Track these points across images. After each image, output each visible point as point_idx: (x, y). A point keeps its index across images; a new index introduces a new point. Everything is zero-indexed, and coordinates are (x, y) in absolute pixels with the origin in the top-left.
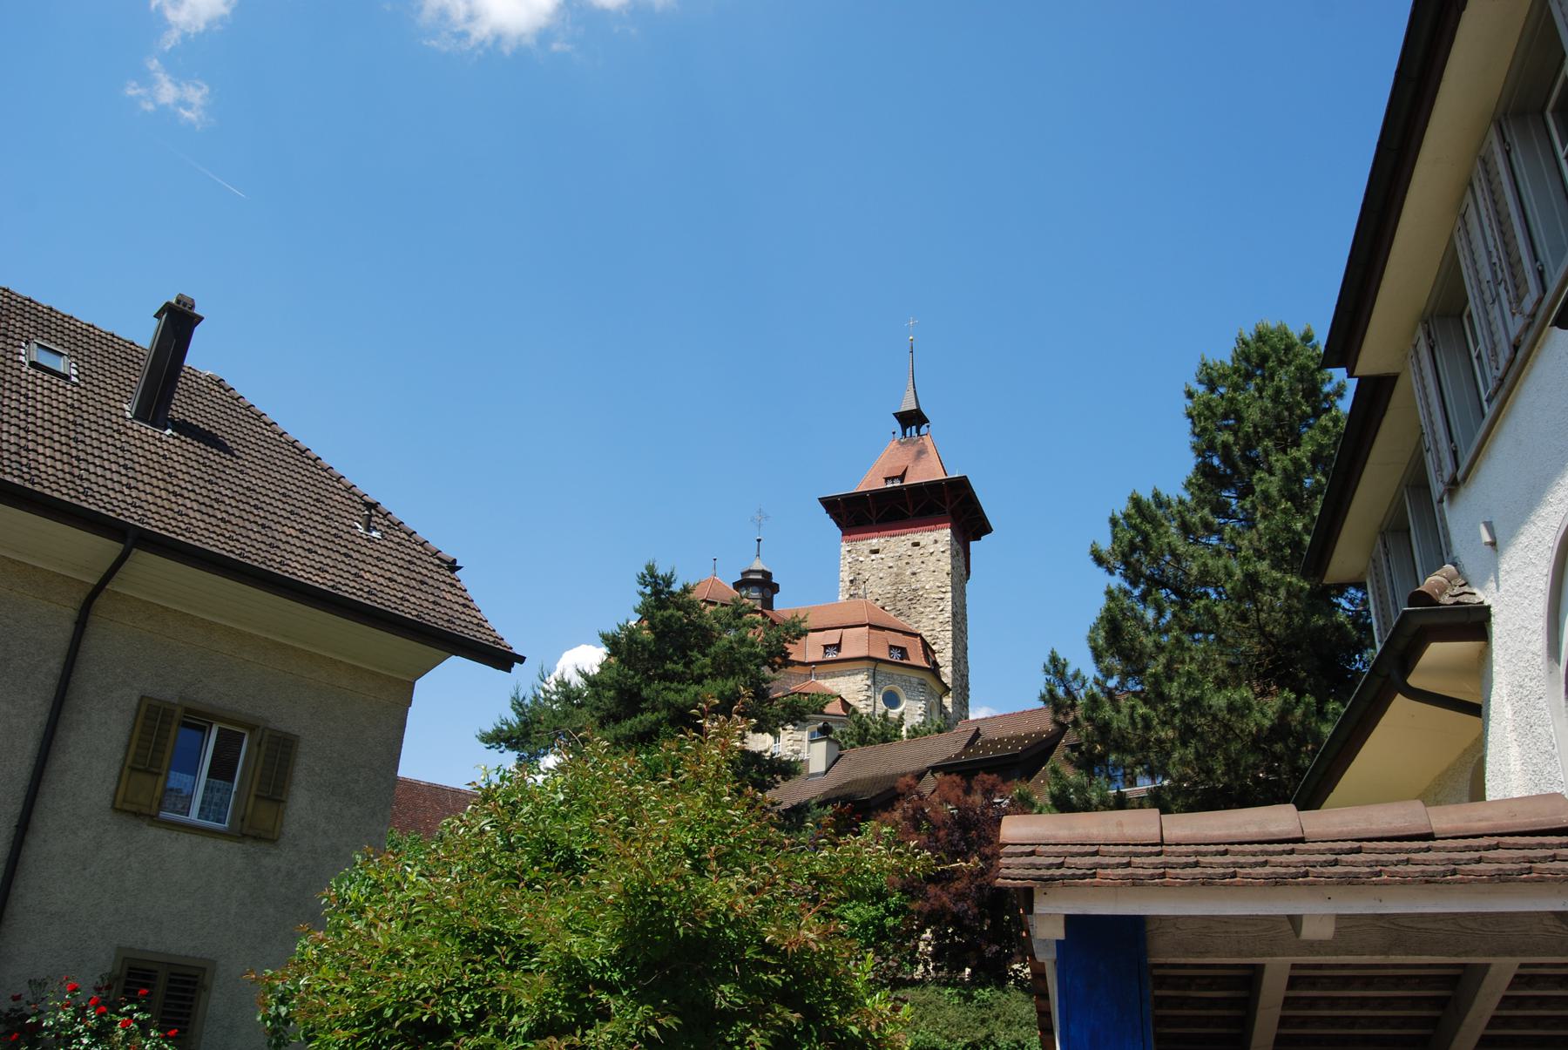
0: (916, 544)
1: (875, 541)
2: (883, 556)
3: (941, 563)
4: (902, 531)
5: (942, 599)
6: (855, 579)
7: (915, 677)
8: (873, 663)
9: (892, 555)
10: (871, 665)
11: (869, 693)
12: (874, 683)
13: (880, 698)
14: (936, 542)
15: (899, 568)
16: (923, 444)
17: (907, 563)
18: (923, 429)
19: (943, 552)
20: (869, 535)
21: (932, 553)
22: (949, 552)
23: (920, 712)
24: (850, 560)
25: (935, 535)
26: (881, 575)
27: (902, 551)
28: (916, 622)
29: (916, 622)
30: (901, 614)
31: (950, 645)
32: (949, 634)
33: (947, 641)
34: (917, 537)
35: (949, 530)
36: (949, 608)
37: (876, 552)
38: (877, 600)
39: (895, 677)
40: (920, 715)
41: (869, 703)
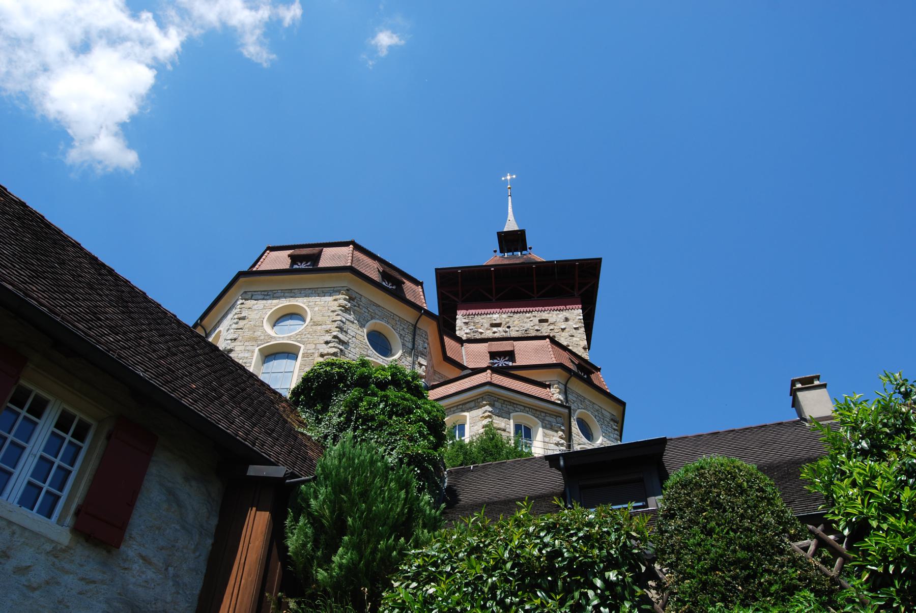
1: (495, 316)
3: (574, 339)
8: (565, 373)
14: (567, 320)
19: (575, 329)
21: (563, 330)
24: (468, 331)
25: (565, 314)
34: (545, 315)
35: (581, 311)
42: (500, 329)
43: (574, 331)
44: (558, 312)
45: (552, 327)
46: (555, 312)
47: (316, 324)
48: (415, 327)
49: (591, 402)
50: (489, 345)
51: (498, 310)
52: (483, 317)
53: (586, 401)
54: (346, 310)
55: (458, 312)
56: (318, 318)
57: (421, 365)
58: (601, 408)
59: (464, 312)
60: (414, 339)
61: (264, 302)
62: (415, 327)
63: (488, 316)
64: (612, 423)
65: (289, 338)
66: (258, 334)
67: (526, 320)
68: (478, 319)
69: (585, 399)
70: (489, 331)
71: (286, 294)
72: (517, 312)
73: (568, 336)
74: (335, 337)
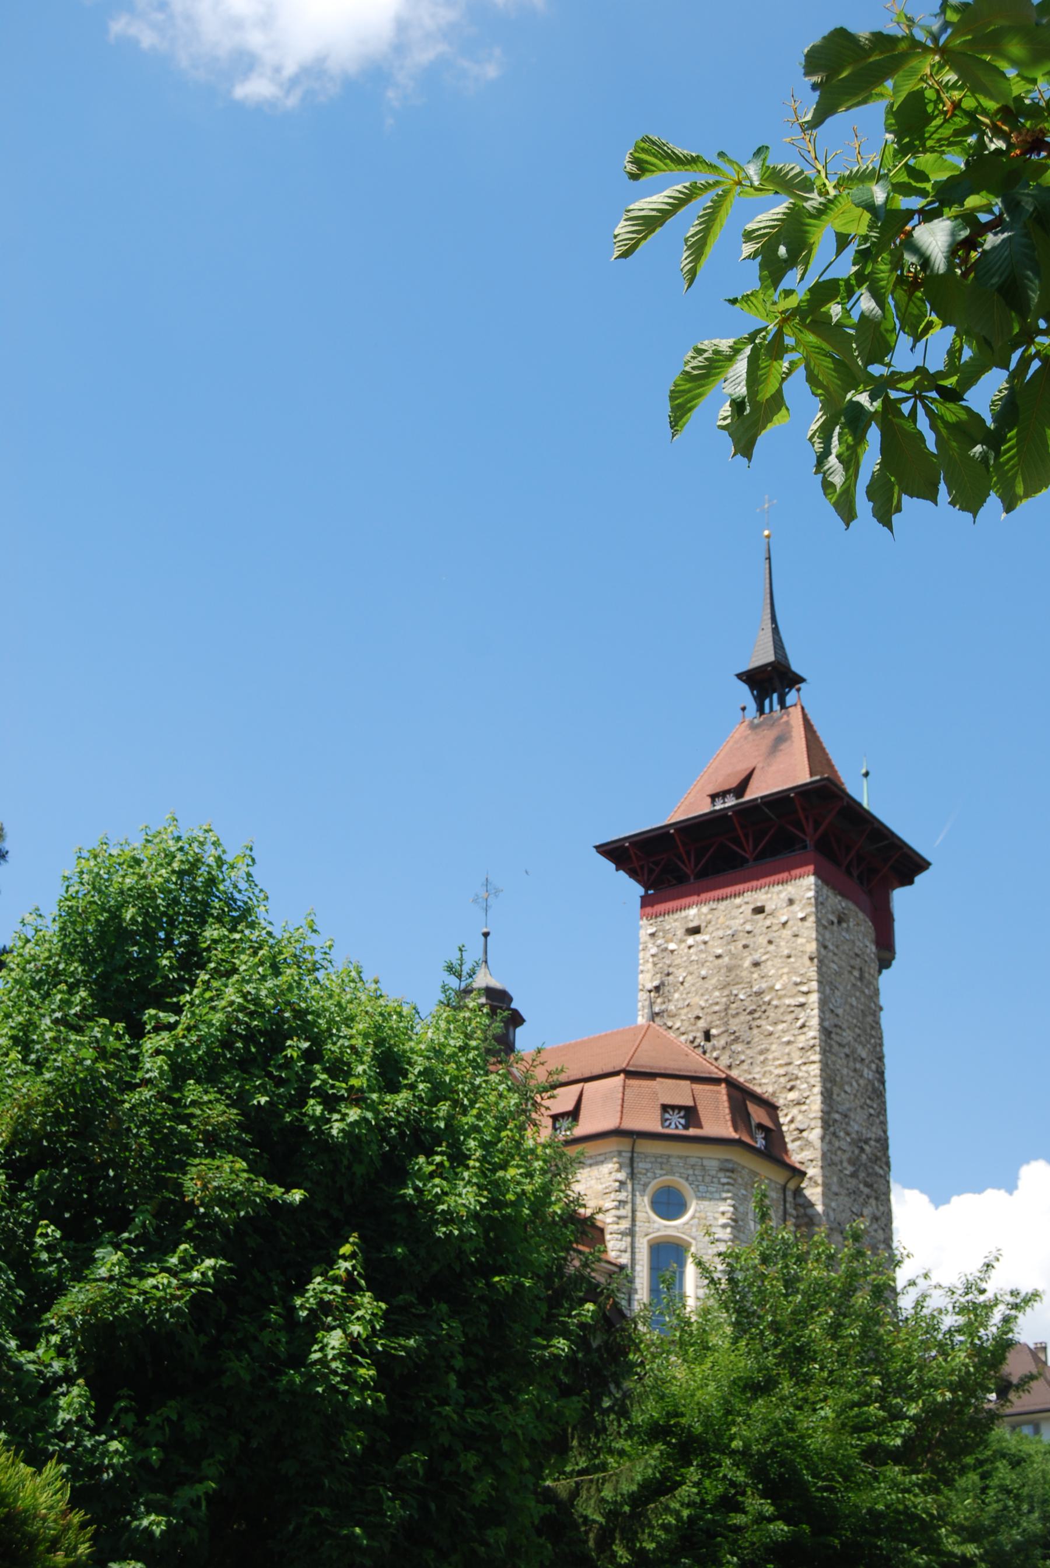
0: (759, 910)
1: (693, 911)
2: (706, 938)
3: (800, 940)
5: (802, 1005)
6: (662, 984)
7: (712, 1157)
9: (720, 933)
10: (625, 1144)
11: (622, 1196)
12: (632, 1175)
13: (644, 1203)
14: (791, 902)
15: (733, 956)
16: (787, 723)
18: (791, 697)
19: (803, 919)
21: (784, 924)
22: (812, 918)
23: (723, 1220)
24: (654, 951)
25: (790, 890)
26: (703, 973)
27: (736, 924)
28: (761, 1053)
29: (761, 1053)
30: (736, 1040)
31: (817, 1090)
32: (815, 1069)
33: (813, 1081)
34: (762, 896)
35: (811, 879)
36: (815, 1022)
37: (695, 931)
38: (698, 1018)
39: (673, 1161)
40: (724, 1226)
41: (622, 1212)
43: (800, 923)
44: (780, 887)
45: (768, 923)
49: (680, 1157)
51: (695, 898)
53: (672, 1160)
58: (702, 1158)
63: (684, 914)
64: (721, 1175)
69: (669, 1156)
73: (789, 937)
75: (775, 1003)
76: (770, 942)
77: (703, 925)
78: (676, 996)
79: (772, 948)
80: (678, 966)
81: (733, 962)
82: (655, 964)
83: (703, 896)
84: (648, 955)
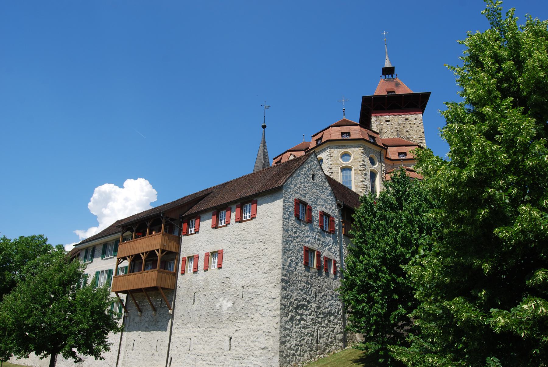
0: (406, 119)
1: (387, 117)
3: (419, 128)
4: (400, 113)
5: (421, 142)
9: (396, 123)
14: (416, 119)
16: (397, 81)
17: (404, 127)
19: (419, 123)
20: (385, 114)
21: (414, 124)
22: (422, 124)
24: (377, 124)
25: (415, 116)
26: (392, 131)
27: (400, 122)
34: (407, 117)
42: (390, 123)
45: (410, 123)
46: (411, 115)
47: (355, 159)
48: (380, 153)
50: (397, 149)
51: (388, 114)
52: (383, 117)
54: (363, 153)
55: (372, 115)
56: (356, 157)
57: (383, 166)
59: (374, 114)
60: (380, 157)
61: (337, 150)
62: (380, 153)
63: (384, 117)
65: (348, 164)
66: (338, 162)
67: (399, 119)
68: (380, 118)
70: (385, 124)
71: (343, 147)
72: (396, 115)
74: (363, 164)
75: (414, 141)
76: (411, 127)
77: (391, 120)
78: (384, 135)
79: (411, 128)
80: (384, 128)
81: (400, 130)
82: (377, 127)
83: (390, 114)
84: (375, 125)
